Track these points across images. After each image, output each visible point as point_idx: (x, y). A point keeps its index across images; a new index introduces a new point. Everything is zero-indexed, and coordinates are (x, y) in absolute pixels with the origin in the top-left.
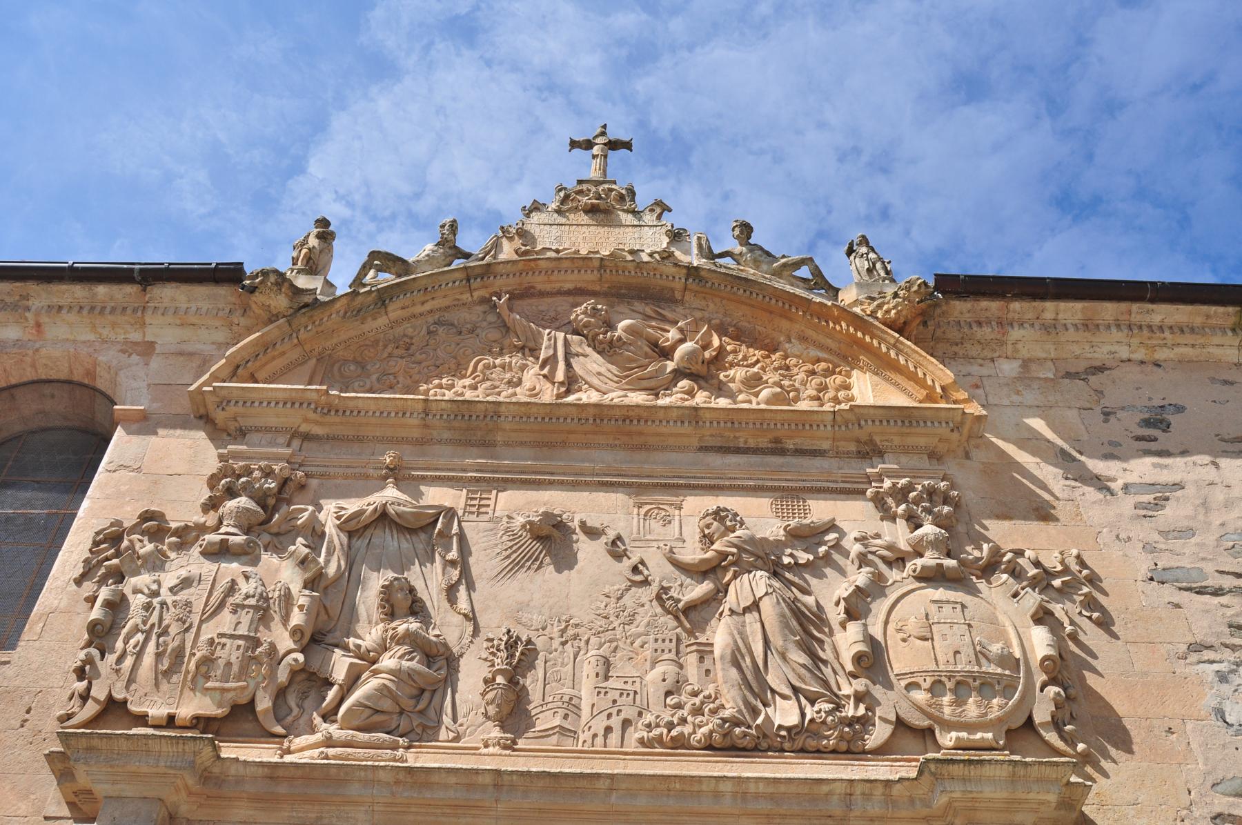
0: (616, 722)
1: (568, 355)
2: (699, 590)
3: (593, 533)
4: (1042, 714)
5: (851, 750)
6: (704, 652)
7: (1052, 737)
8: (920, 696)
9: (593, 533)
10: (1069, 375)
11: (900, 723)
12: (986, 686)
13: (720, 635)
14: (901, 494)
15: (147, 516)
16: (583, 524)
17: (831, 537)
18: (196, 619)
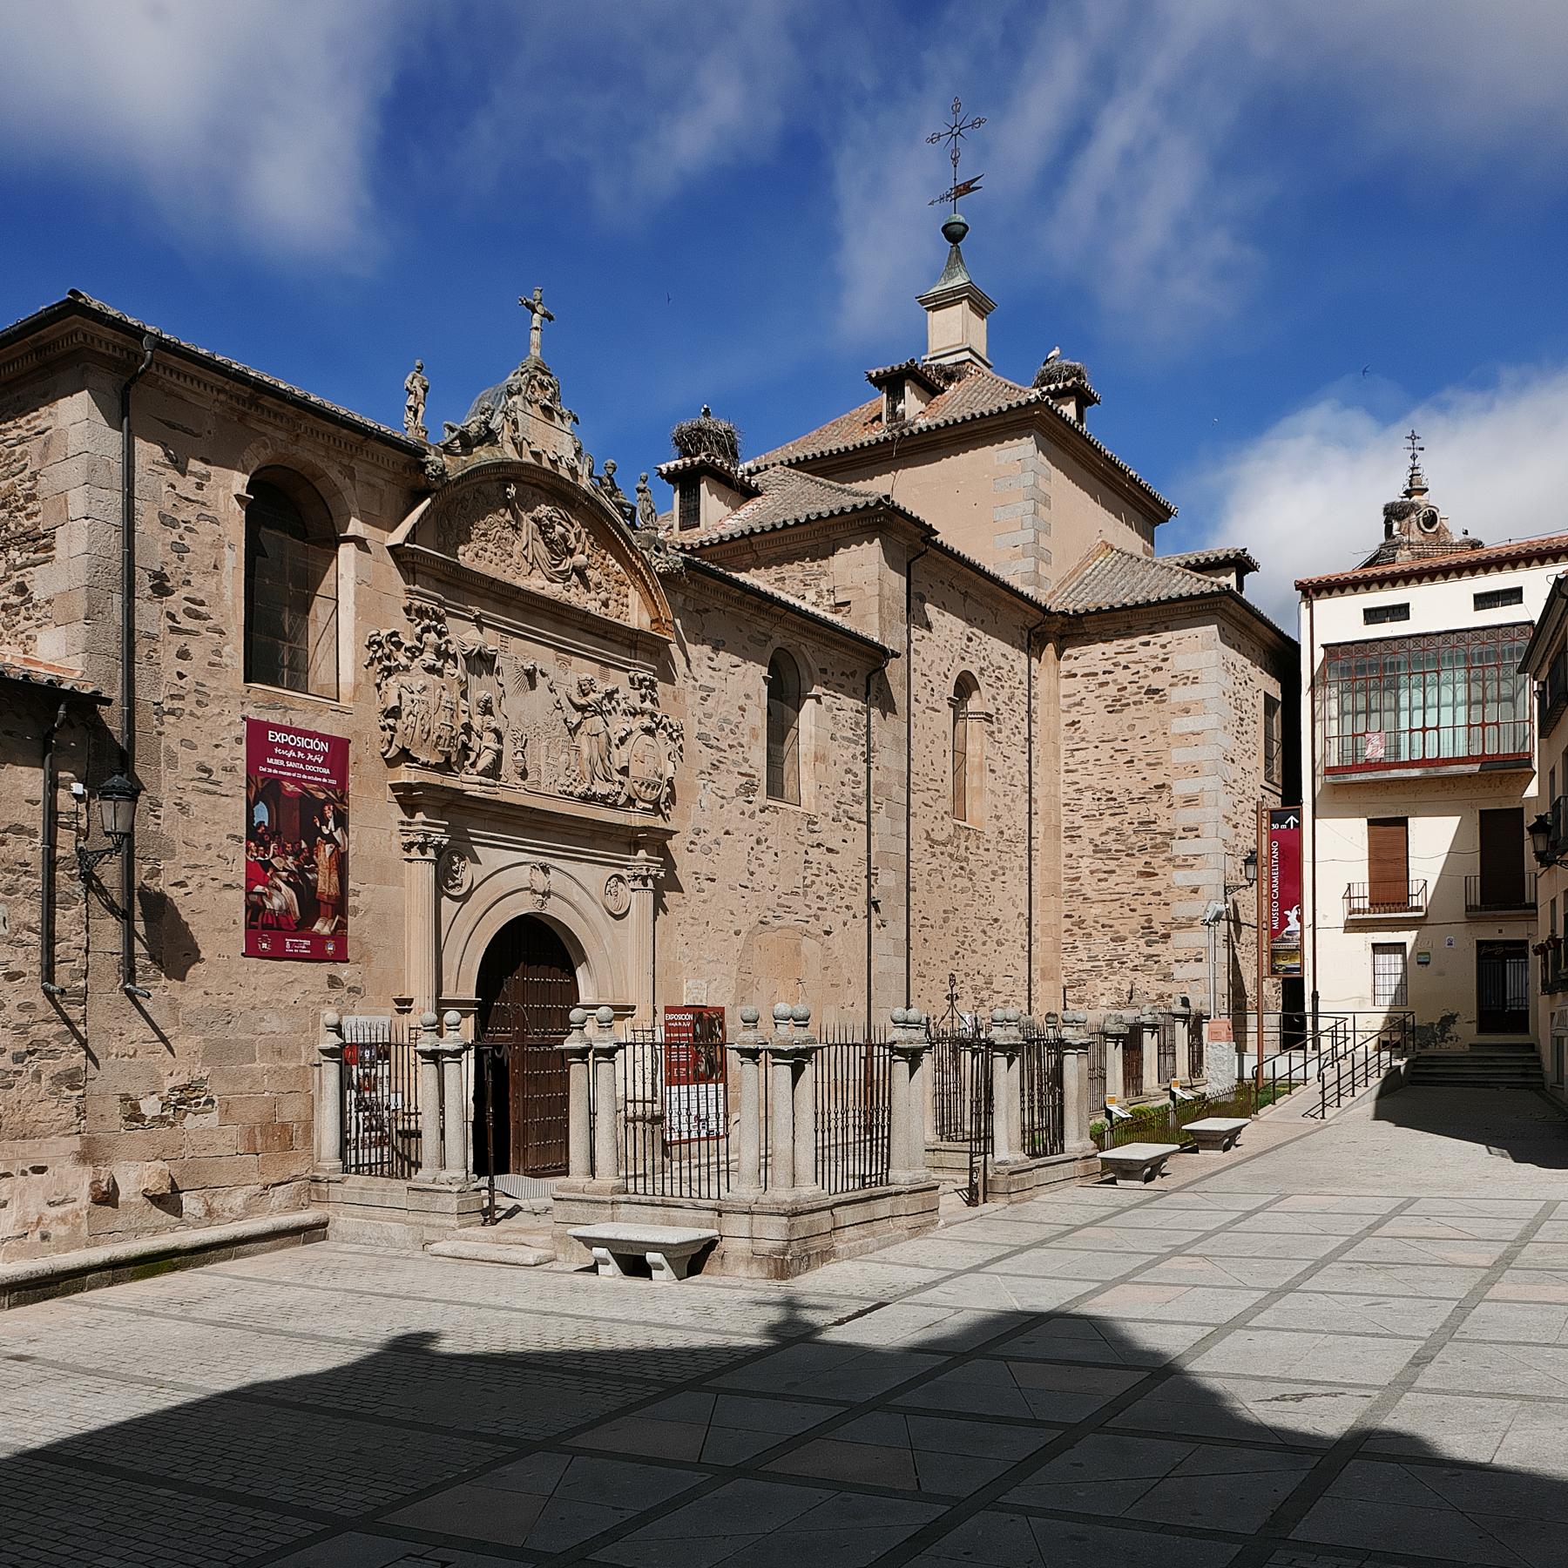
0: (552, 780)
1: (534, 539)
2: (575, 718)
3: (543, 675)
4: (662, 800)
5: (614, 805)
6: (578, 750)
7: (662, 806)
8: (636, 786)
9: (543, 675)
10: (697, 611)
11: (629, 798)
12: (656, 786)
13: (582, 741)
14: (642, 681)
15: (395, 634)
16: (541, 672)
17: (616, 696)
18: (432, 712)
